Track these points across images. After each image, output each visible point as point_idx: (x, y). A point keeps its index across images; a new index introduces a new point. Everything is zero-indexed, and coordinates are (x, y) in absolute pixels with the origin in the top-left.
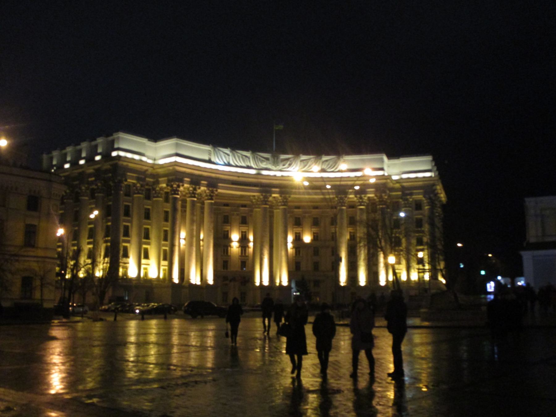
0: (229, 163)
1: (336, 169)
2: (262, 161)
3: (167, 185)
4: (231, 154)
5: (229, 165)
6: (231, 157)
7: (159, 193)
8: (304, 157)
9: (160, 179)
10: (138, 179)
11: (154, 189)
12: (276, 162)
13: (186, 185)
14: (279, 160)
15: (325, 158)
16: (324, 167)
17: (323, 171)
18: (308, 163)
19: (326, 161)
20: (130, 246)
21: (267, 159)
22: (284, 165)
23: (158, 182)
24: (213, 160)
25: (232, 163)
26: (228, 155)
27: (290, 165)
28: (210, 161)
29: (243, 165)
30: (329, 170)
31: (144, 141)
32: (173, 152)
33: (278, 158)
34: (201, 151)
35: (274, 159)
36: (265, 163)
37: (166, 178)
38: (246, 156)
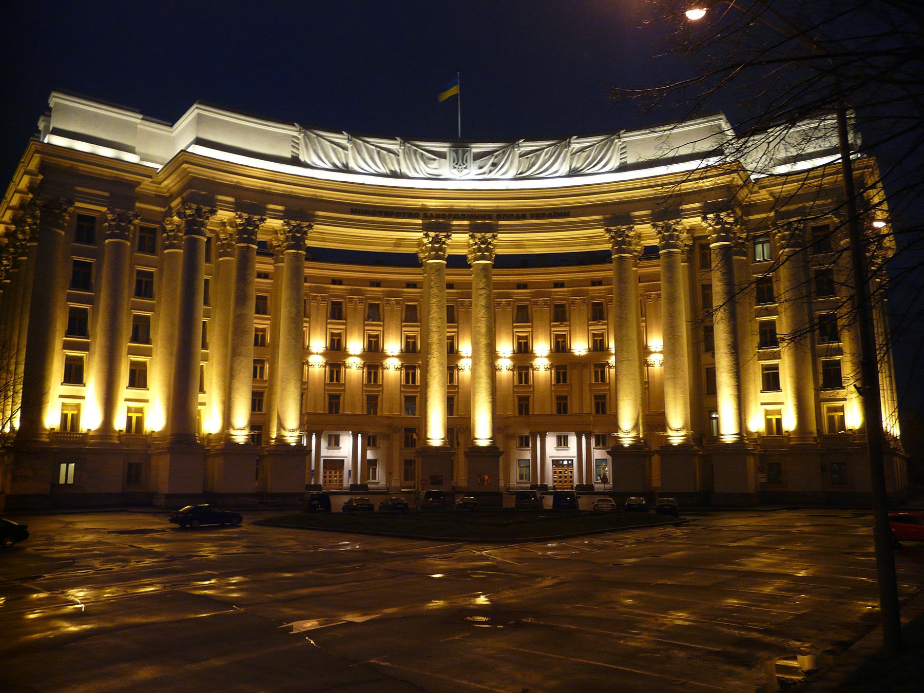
1: (604, 166)
2: (426, 161)
4: (349, 145)
5: (346, 169)
6: (350, 153)
7: (175, 237)
8: (527, 146)
10: (110, 203)
12: (460, 161)
14: (470, 157)
15: (577, 144)
17: (573, 173)
18: (538, 157)
19: (582, 150)
20: (89, 356)
21: (442, 155)
22: (481, 168)
24: (303, 158)
25: (352, 165)
26: (344, 148)
27: (494, 165)
28: (295, 161)
29: (383, 170)
31: (135, 119)
34: (276, 137)
35: (457, 152)
36: (435, 164)
38: (389, 151)
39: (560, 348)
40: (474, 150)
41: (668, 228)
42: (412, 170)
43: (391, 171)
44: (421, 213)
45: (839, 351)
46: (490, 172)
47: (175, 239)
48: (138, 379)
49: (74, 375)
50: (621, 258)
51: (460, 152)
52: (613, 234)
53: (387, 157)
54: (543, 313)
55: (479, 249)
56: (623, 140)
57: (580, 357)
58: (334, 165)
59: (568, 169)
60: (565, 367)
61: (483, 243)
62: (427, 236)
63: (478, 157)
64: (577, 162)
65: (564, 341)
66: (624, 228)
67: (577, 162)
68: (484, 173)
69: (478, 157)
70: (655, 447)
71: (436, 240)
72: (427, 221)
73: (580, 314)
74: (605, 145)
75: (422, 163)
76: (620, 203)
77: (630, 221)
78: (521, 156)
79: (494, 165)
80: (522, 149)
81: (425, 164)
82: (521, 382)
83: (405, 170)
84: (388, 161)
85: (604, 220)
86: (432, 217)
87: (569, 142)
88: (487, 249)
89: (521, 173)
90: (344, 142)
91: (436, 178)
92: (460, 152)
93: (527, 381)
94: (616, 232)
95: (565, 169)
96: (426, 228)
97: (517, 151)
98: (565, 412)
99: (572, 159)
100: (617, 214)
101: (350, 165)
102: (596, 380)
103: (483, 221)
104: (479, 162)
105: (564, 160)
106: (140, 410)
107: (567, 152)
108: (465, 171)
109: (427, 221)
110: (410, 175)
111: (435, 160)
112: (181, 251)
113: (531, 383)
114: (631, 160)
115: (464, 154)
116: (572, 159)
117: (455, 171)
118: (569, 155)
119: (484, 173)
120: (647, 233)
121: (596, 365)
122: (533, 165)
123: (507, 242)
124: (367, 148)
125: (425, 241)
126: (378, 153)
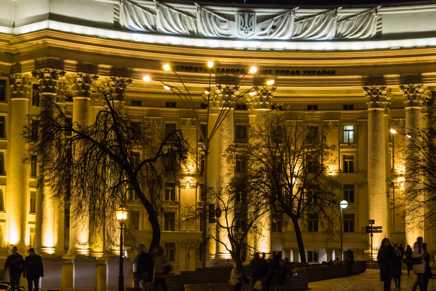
0: (155, 28)
1: (364, 34)
2: (219, 23)
3: (34, 74)
4: (158, 11)
5: (155, 31)
6: (158, 17)
7: (22, 88)
8: (300, 12)
9: (22, 63)
11: (12, 81)
12: (246, 25)
13: (68, 73)
14: (254, 20)
15: (342, 13)
16: (342, 30)
17: (339, 38)
18: (310, 22)
19: (347, 18)
21: (231, 18)
22: (263, 29)
23: (18, 69)
29: (184, 31)
30: (348, 37)
32: (44, 11)
33: (249, 17)
35: (243, 16)
36: (225, 26)
37: (32, 61)
38: (189, 14)
40: (257, 14)
41: (412, 90)
42: (207, 31)
43: (190, 31)
46: (271, 33)
47: (22, 90)
50: (375, 111)
51: (246, 16)
52: (369, 91)
53: (187, 20)
55: (261, 99)
56: (379, 13)
59: (334, 34)
61: (264, 94)
62: (220, 88)
63: (261, 20)
64: (342, 29)
66: (378, 87)
67: (342, 29)
68: (265, 34)
69: (261, 20)
72: (219, 75)
74: (365, 16)
75: (215, 25)
76: (376, 66)
77: (382, 81)
78: (296, 20)
79: (274, 27)
80: (297, 15)
81: (218, 25)
83: (201, 30)
84: (188, 23)
85: (363, 79)
87: (336, 12)
88: (267, 99)
89: (296, 35)
90: (154, 8)
91: (226, 38)
92: (246, 16)
94: (372, 90)
95: (331, 35)
97: (293, 17)
99: (338, 25)
100: (373, 76)
101: (158, 27)
104: (261, 25)
105: (331, 27)
107: (334, 20)
108: (251, 33)
110: (205, 35)
111: (225, 22)
112: (27, 100)
114: (385, 31)
115: (249, 18)
116: (338, 25)
117: (242, 32)
118: (335, 22)
119: (265, 34)
122: (306, 29)
124: (171, 12)
125: (218, 91)
126: (180, 16)
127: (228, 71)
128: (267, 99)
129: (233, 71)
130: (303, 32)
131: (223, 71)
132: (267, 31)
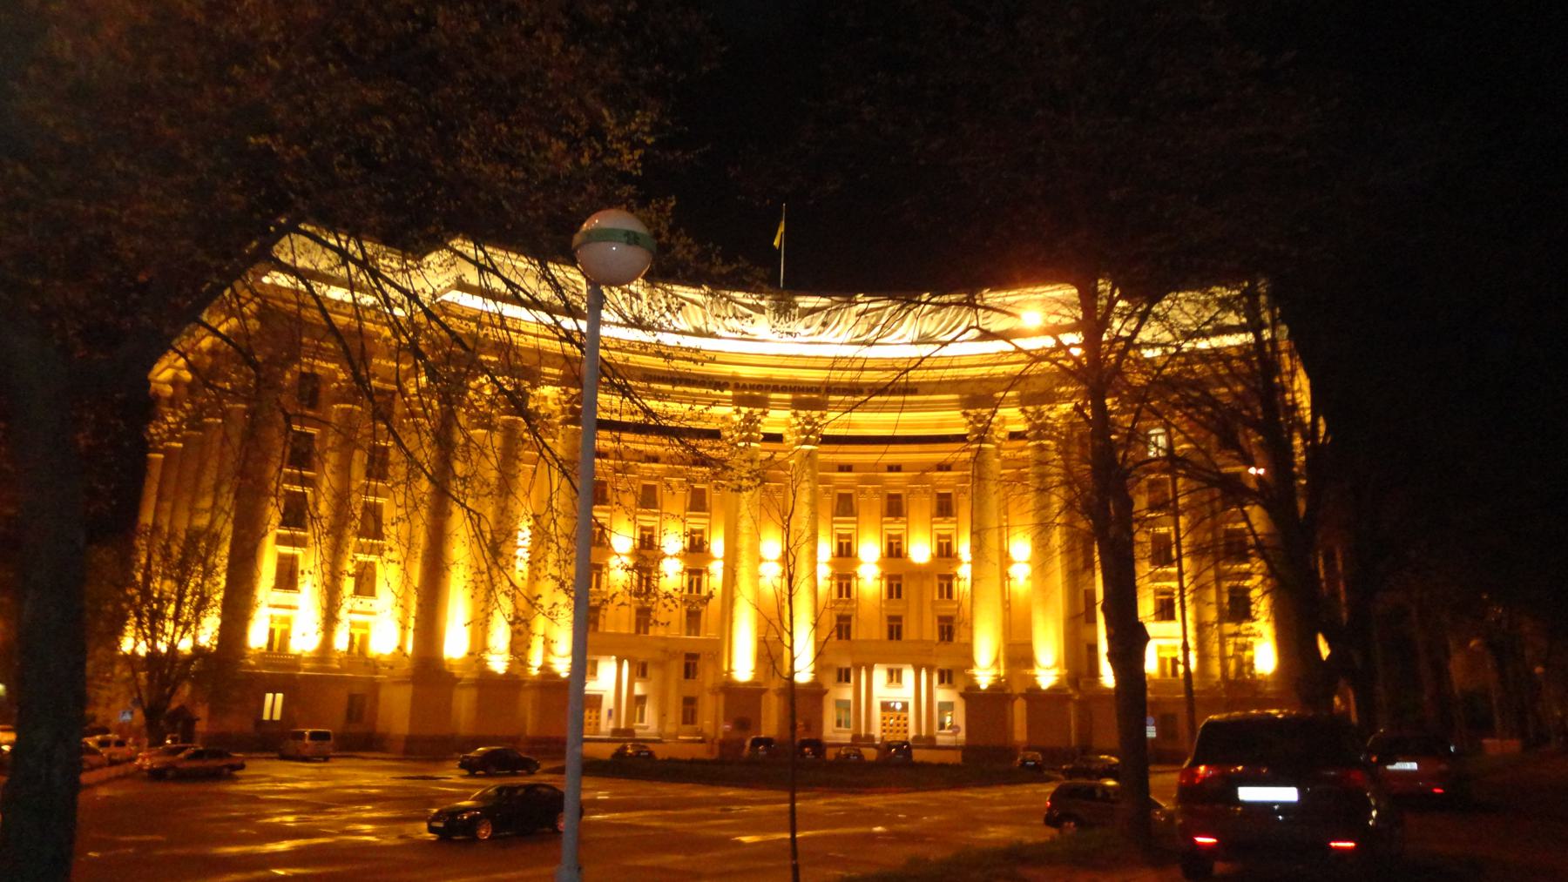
17: (924, 339)
21: (761, 310)
27: (824, 324)
39: (894, 551)
44: (732, 383)
45: (1248, 575)
48: (365, 583)
49: (287, 577)
54: (869, 504)
55: (803, 431)
57: (920, 567)
58: (625, 318)
60: (899, 577)
62: (738, 412)
65: (899, 543)
70: (1018, 688)
71: (750, 419)
72: (739, 393)
73: (921, 506)
76: (981, 381)
79: (824, 324)
82: (840, 595)
84: (692, 315)
85: (960, 400)
86: (744, 387)
88: (813, 432)
93: (848, 595)
96: (738, 401)
98: (899, 637)
102: (941, 596)
103: (809, 396)
106: (365, 626)
109: (739, 393)
113: (854, 595)
120: (1012, 417)
121: (941, 577)
122: (873, 326)
123: (835, 421)
127: (752, 388)
128: (813, 432)
129: (759, 388)
130: (869, 331)
131: (744, 387)
132: (813, 329)
